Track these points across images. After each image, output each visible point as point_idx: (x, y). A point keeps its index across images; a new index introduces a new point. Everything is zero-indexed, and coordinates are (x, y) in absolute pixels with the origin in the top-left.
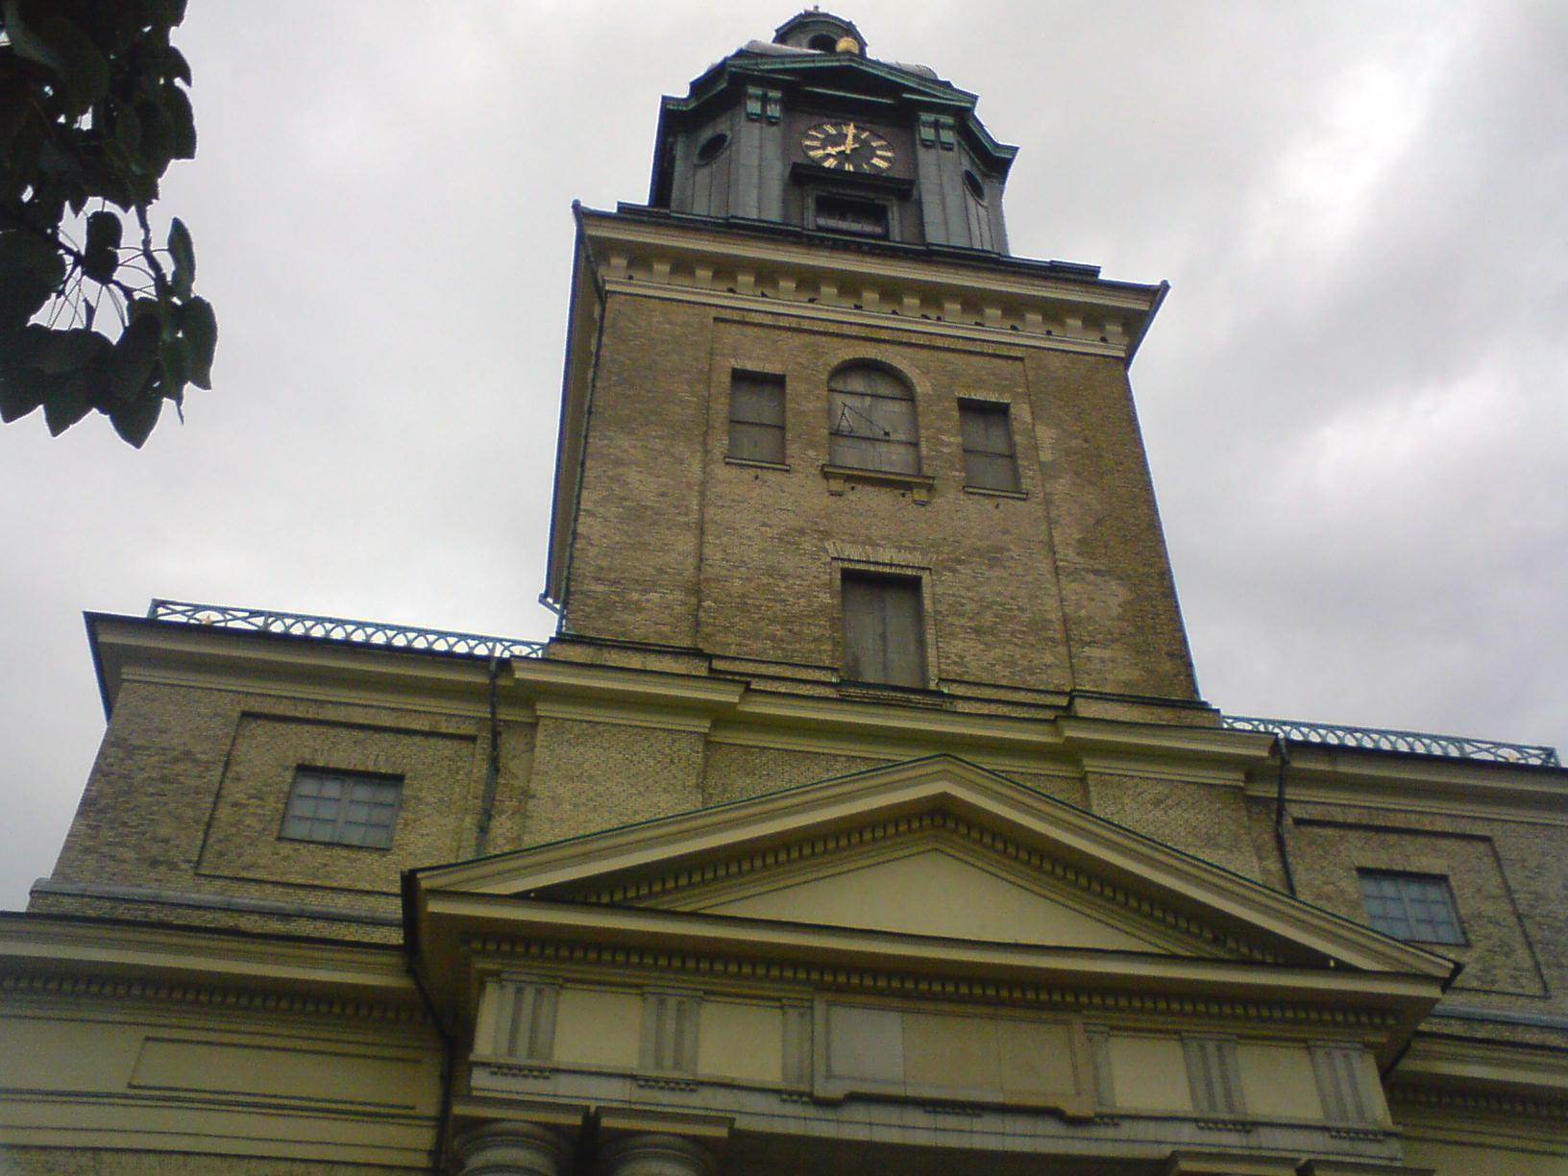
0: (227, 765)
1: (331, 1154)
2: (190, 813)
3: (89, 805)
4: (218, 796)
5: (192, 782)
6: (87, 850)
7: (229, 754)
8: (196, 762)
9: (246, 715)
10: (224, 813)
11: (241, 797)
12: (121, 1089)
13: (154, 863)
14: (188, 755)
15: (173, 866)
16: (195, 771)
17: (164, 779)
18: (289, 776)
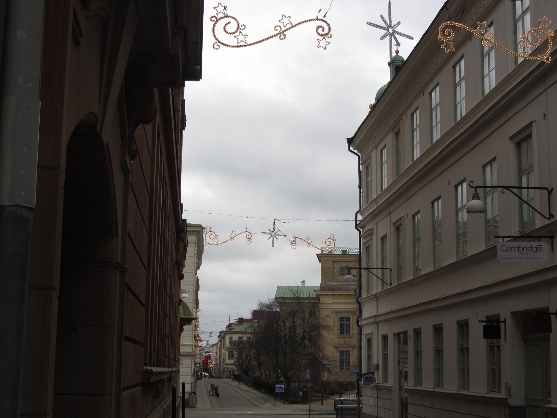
0: (333, 268)
1: (351, 308)
2: (331, 274)
3: (322, 275)
4: (333, 272)
5: (330, 271)
6: (323, 280)
7: (333, 267)
8: (330, 268)
9: (334, 262)
10: (334, 273)
11: (335, 272)
12: (332, 303)
13: (329, 280)
14: (329, 267)
15: (331, 280)
16: (331, 269)
17: (328, 271)
18: (339, 268)
